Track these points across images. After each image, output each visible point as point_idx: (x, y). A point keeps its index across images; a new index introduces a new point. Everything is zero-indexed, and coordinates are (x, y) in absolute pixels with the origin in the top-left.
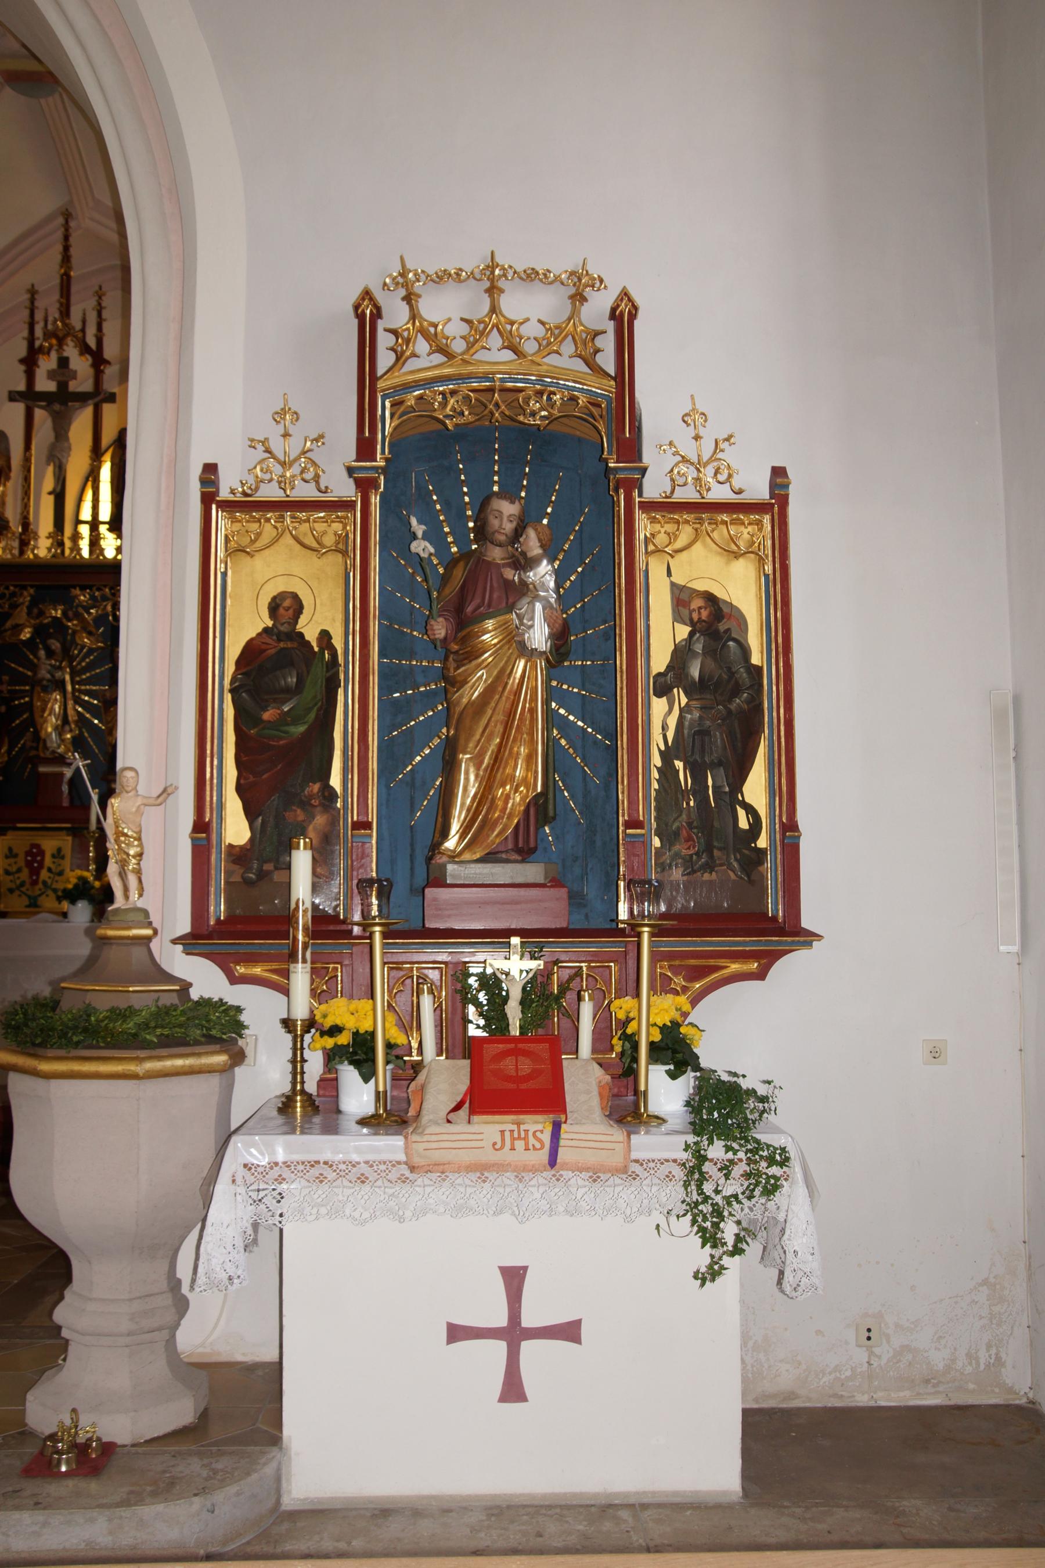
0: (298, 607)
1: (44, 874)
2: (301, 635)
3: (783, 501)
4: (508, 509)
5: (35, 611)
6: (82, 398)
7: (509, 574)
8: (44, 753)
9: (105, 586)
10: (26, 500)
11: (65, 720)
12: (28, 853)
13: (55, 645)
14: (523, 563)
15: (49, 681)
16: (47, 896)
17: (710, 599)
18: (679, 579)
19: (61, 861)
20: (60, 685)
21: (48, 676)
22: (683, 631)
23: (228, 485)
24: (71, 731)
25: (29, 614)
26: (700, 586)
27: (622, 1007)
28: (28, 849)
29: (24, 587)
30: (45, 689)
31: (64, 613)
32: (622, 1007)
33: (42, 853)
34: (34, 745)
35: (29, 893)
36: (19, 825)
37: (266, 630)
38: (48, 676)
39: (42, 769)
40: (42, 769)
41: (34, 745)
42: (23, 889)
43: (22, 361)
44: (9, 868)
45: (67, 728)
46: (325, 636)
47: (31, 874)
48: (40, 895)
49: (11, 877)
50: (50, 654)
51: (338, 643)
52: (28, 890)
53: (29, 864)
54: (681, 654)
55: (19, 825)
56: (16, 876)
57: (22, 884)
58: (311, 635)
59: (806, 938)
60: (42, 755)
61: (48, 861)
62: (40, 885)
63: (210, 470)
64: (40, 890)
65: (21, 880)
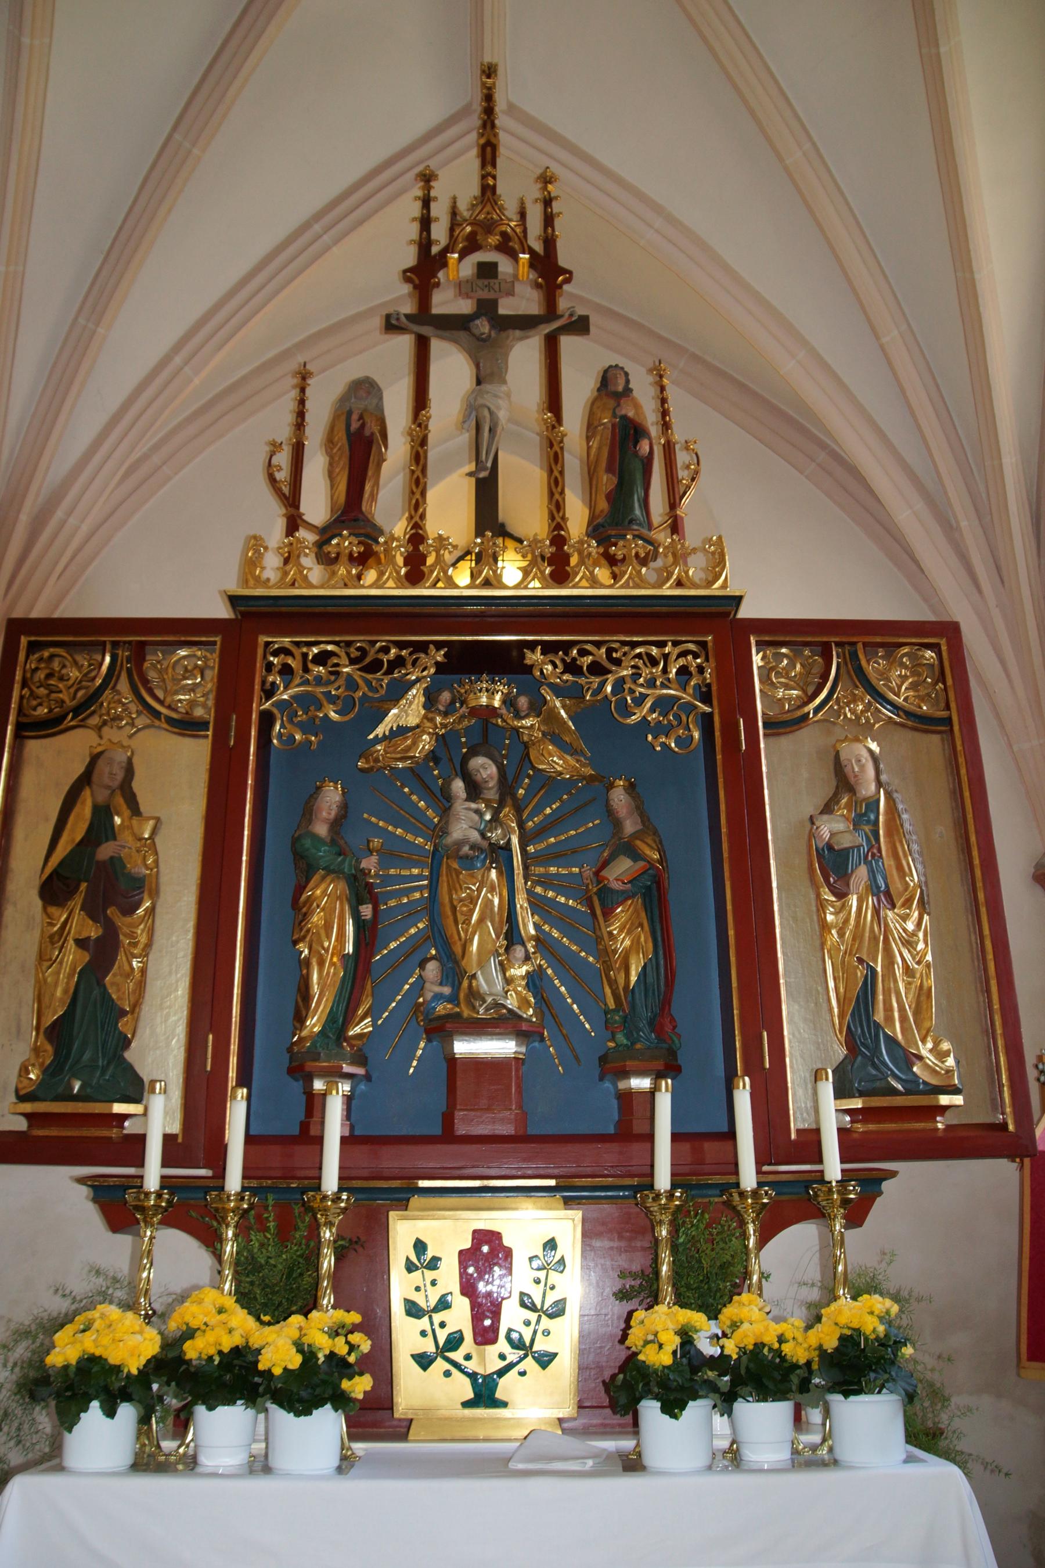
5: (446, 696)
6: (525, 323)
8: (474, 1008)
9: (598, 644)
10: (418, 496)
11: (512, 936)
12: (465, 1257)
15: (473, 847)
16: (523, 1374)
19: (554, 1277)
20: (499, 854)
21: (475, 836)
24: (527, 958)
25: (430, 702)
28: (467, 1244)
30: (467, 862)
31: (509, 702)
34: (447, 990)
35: (471, 1366)
36: (423, 1184)
38: (475, 836)
39: (463, 1047)
40: (463, 1047)
41: (447, 990)
42: (457, 1356)
43: (408, 275)
44: (419, 1299)
45: (519, 952)
47: (477, 1318)
48: (502, 1373)
49: (424, 1323)
50: (474, 790)
52: (468, 1357)
53: (468, 1288)
55: (423, 1184)
56: (437, 1318)
57: (455, 1341)
60: (466, 1013)
64: (502, 1357)
65: (449, 1329)
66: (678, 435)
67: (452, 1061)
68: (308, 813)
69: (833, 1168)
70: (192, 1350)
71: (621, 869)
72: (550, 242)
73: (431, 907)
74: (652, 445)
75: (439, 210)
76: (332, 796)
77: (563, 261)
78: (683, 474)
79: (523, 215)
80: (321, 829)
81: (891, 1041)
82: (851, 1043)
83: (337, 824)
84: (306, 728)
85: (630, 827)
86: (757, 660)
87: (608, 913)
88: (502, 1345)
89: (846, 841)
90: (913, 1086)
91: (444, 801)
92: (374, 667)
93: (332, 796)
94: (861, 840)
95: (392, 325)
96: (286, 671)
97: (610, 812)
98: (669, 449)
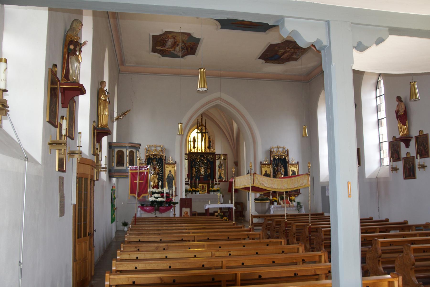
0: (267, 171)
1: (204, 189)
2: (267, 174)
3: (298, 164)
4: (280, 164)
7: (280, 169)
12: (202, 186)
13: (202, 162)
14: (281, 168)
17: (294, 171)
18: (292, 169)
22: (292, 173)
23: (263, 163)
26: (293, 170)
27: (291, 198)
29: (199, 155)
30: (201, 167)
31: (203, 158)
32: (291, 198)
33: (204, 186)
37: (265, 173)
46: (269, 173)
50: (201, 163)
51: (270, 174)
53: (202, 188)
54: (292, 174)
58: (268, 173)
59: (300, 194)
61: (204, 187)
62: (204, 190)
63: (261, 162)
66: (213, 140)
67: (200, 177)
68: (192, 164)
69: (218, 182)
70: (193, 190)
71: (209, 167)
72: (206, 126)
73: (199, 168)
74: (211, 142)
75: (199, 122)
76: (193, 163)
77: (207, 127)
78: (213, 143)
79: (204, 123)
80: (193, 165)
81: (222, 177)
82: (219, 177)
83: (194, 164)
84: (193, 160)
85: (209, 165)
86: (216, 156)
87: (208, 170)
88: (204, 190)
89: (220, 166)
90: (222, 179)
91: (200, 163)
92: (196, 156)
93: (193, 163)
94: (221, 166)
95: (196, 132)
96: (191, 156)
97: (208, 163)
98: (212, 141)
